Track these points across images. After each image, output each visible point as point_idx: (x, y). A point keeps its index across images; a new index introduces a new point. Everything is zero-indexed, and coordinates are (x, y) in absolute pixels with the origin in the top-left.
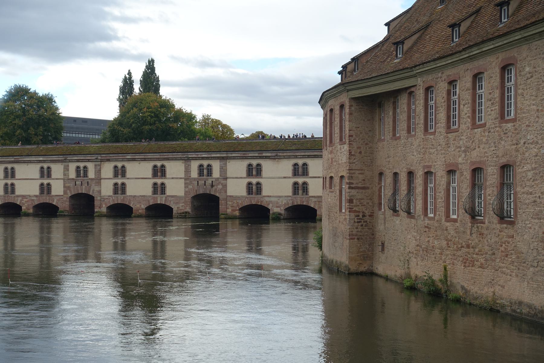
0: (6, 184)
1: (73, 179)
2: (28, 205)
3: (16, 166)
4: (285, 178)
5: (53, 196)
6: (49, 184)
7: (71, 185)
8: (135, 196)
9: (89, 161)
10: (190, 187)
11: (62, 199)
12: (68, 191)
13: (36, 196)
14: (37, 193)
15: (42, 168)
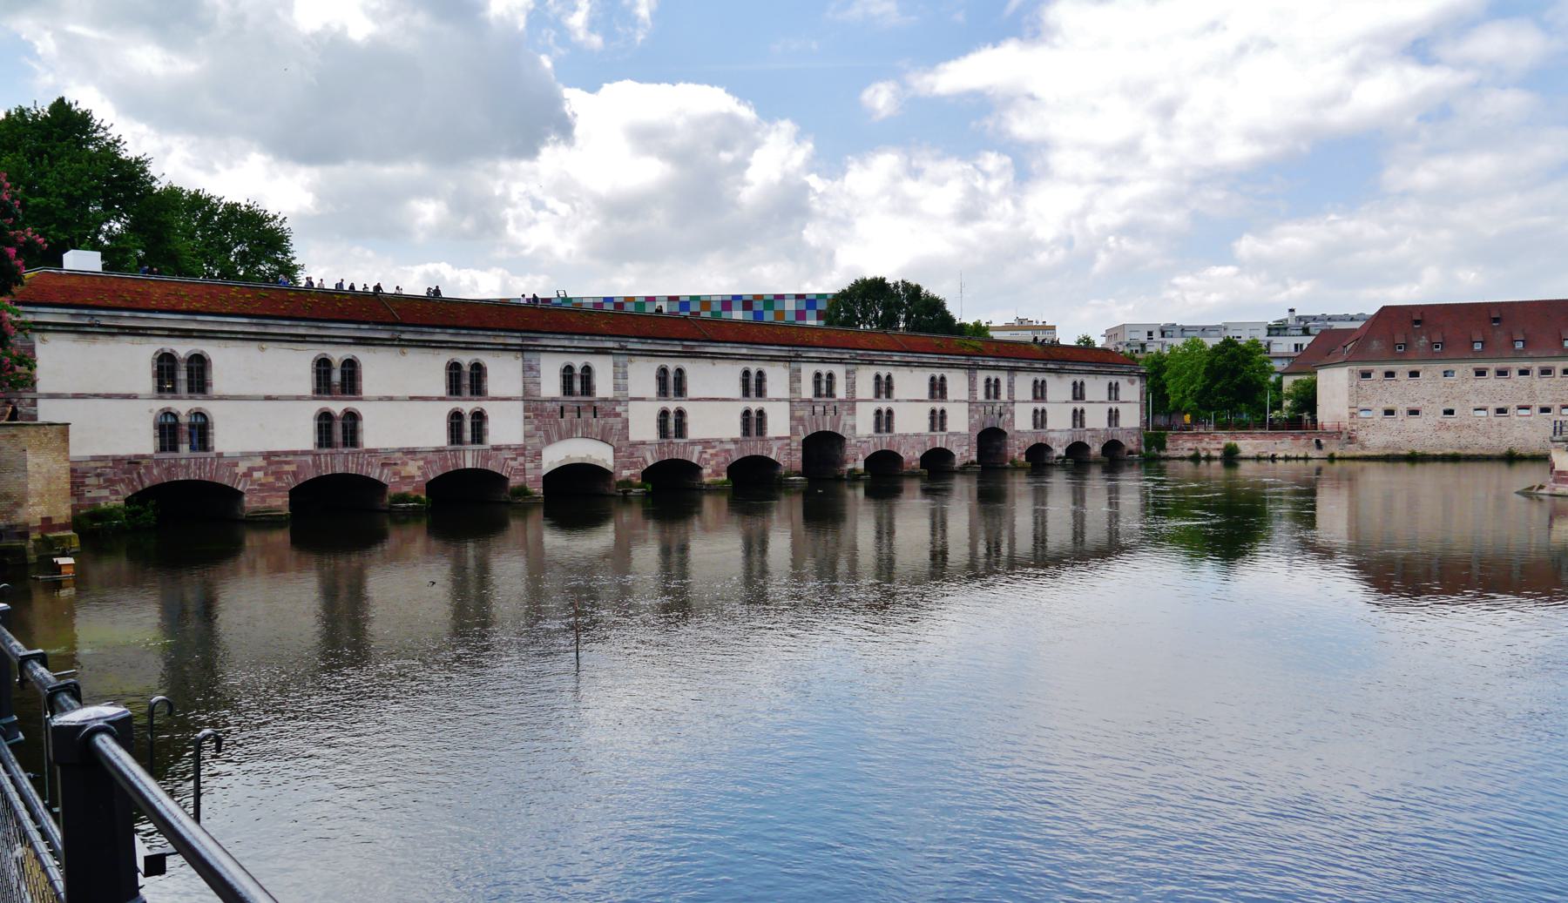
0: (664, 414)
1: (810, 401)
2: (718, 464)
3: (686, 364)
4: (1067, 402)
5: (771, 439)
6: (761, 413)
7: (805, 413)
8: (907, 435)
9: (841, 363)
10: (977, 417)
11: (789, 445)
12: (801, 428)
13: (735, 441)
14: (737, 432)
15: (746, 373)
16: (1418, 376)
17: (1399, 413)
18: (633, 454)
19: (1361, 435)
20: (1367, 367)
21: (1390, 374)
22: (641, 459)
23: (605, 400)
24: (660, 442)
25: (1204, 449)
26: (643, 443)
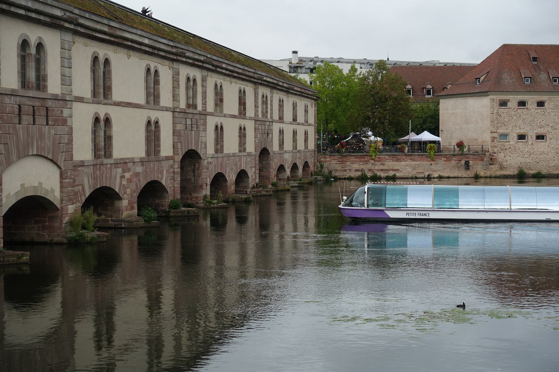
13: (142, 162)
16: (544, 106)
17: (529, 137)
18: (74, 181)
19: (500, 157)
20: (504, 97)
21: (522, 104)
22: (80, 187)
23: (55, 98)
24: (95, 163)
25: (370, 170)
26: (82, 164)
